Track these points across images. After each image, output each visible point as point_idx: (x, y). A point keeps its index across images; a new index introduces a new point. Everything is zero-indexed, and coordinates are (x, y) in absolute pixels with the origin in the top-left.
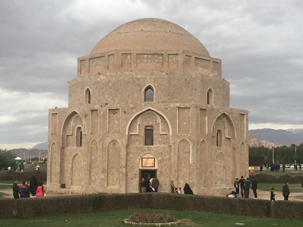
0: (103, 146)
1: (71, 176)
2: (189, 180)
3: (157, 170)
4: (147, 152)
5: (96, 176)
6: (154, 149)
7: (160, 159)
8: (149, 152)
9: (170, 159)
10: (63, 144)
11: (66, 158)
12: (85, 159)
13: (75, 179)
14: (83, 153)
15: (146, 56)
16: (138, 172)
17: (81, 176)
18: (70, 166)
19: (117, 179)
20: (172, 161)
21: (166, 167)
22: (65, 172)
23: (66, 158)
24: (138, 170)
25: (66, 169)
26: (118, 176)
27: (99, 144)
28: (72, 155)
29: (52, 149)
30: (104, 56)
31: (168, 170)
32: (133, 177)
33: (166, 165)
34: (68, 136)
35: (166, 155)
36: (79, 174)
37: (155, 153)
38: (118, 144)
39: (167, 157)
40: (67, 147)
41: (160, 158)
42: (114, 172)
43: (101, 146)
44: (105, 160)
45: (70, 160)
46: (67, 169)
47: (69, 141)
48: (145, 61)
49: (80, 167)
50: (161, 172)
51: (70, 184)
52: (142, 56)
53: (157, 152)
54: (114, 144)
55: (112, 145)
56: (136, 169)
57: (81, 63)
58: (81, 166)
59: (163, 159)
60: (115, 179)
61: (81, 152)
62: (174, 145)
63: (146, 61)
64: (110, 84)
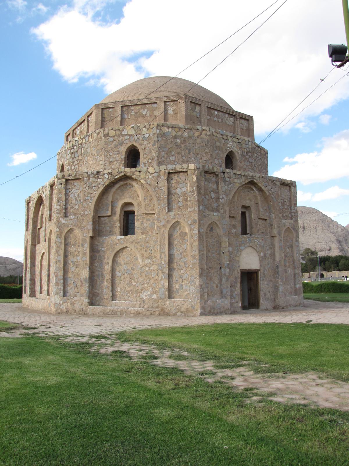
0: (199, 231)
1: (110, 285)
2: (295, 284)
3: (259, 270)
4: (248, 244)
5: (182, 281)
6: (256, 241)
7: (262, 255)
8: (251, 244)
9: (273, 255)
10: (94, 230)
11: (98, 255)
12: (146, 254)
13: (119, 289)
14: (141, 246)
15: (216, 113)
16: (239, 274)
17: (134, 283)
18: (108, 268)
19: (217, 287)
20: (277, 259)
21: (269, 266)
22: (96, 278)
23: (98, 255)
24: (239, 271)
25: (97, 273)
26: (218, 281)
27: (191, 228)
28: (113, 249)
29: (65, 239)
30: (156, 103)
31: (271, 271)
32: (234, 282)
33: (269, 264)
34: (99, 217)
35: (268, 250)
36: (131, 282)
37: (257, 246)
38: (218, 230)
39: (269, 252)
40: (99, 235)
41: (262, 254)
42: (213, 274)
43: (196, 231)
44: (203, 254)
45: (108, 258)
46: (100, 273)
47: (103, 226)
48: (215, 119)
49: (133, 269)
50: (264, 274)
51: (111, 299)
52: (213, 111)
53: (259, 245)
54: (212, 229)
55: (210, 231)
56: (237, 270)
57: (102, 113)
58: (134, 267)
59: (265, 255)
60: (215, 286)
61: (136, 243)
62: (280, 235)
63: (217, 120)
64: (178, 141)
